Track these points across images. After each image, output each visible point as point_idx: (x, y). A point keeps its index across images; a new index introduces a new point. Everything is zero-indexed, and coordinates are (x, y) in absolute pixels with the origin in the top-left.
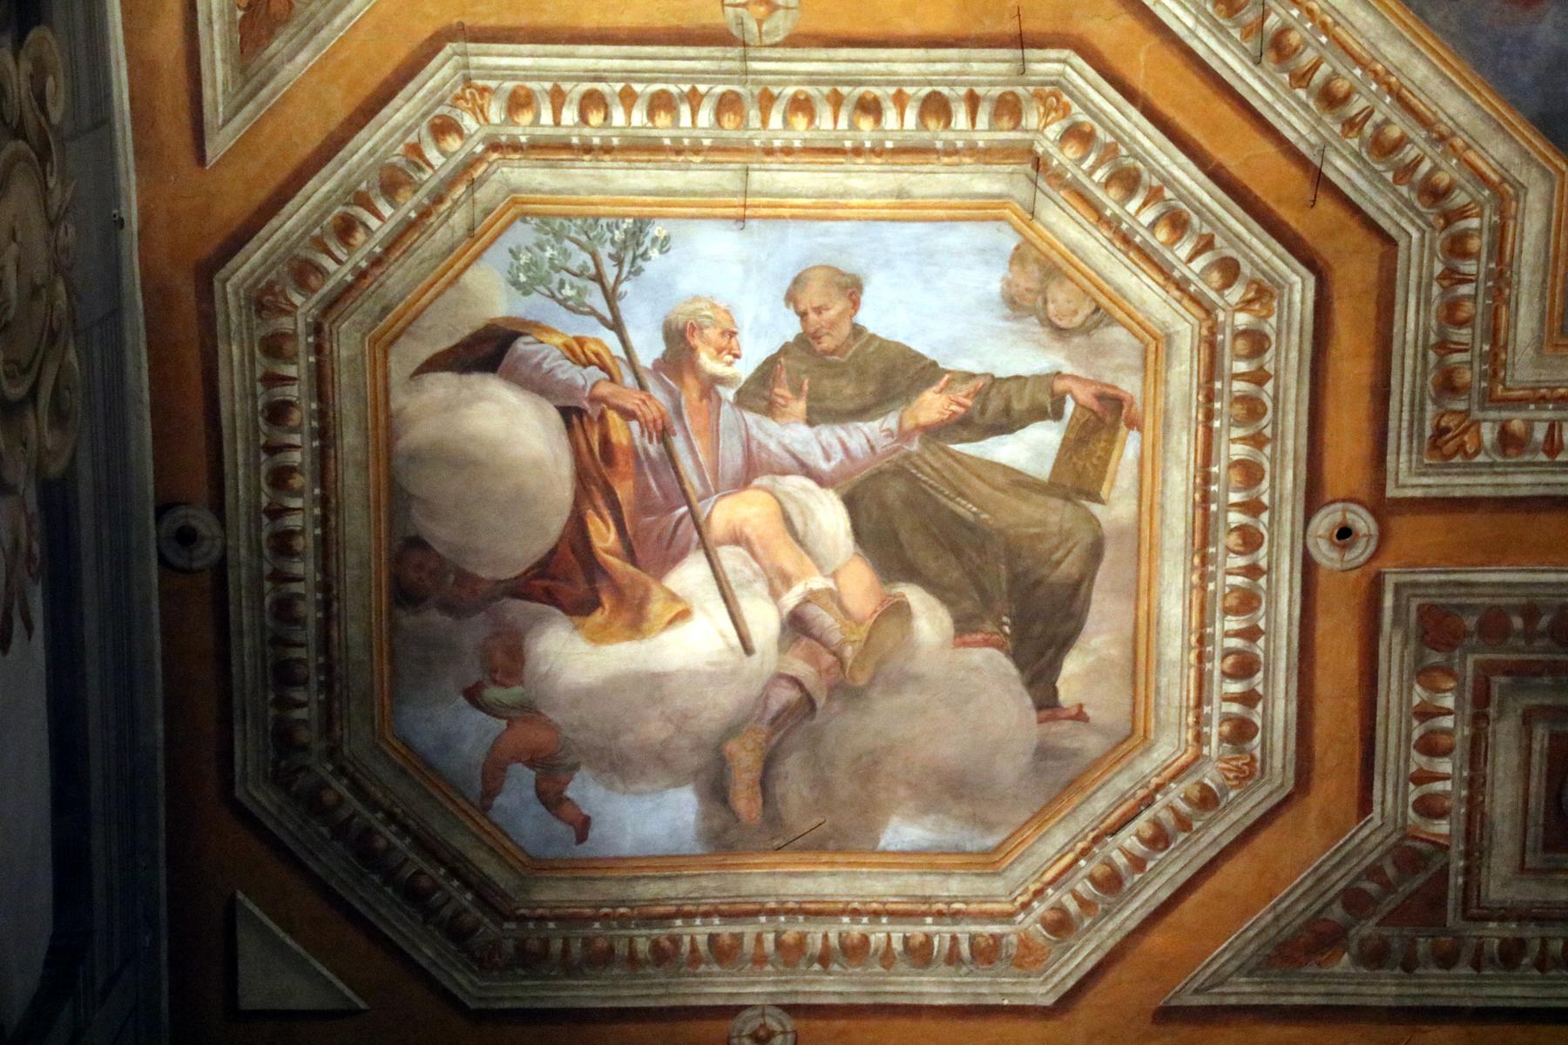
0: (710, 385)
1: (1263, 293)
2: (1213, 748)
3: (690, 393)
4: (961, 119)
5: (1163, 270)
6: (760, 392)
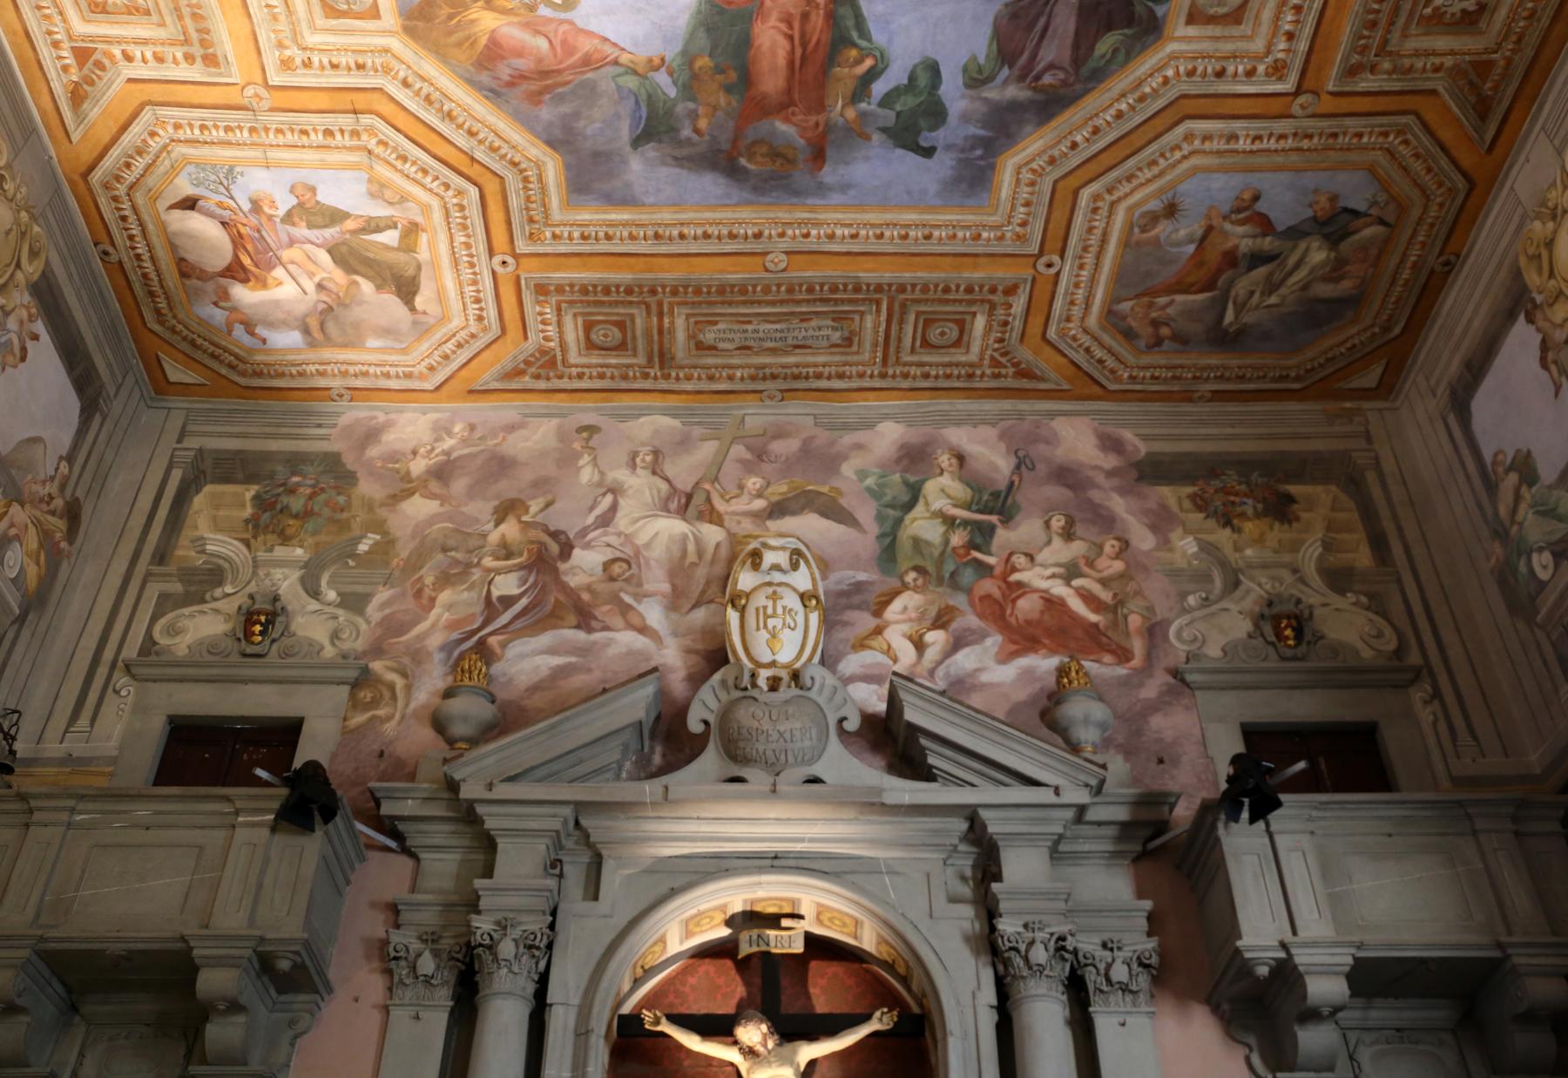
0: (270, 218)
1: (460, 193)
2: (472, 322)
3: (264, 220)
4: (338, 136)
5: (423, 186)
6: (288, 218)
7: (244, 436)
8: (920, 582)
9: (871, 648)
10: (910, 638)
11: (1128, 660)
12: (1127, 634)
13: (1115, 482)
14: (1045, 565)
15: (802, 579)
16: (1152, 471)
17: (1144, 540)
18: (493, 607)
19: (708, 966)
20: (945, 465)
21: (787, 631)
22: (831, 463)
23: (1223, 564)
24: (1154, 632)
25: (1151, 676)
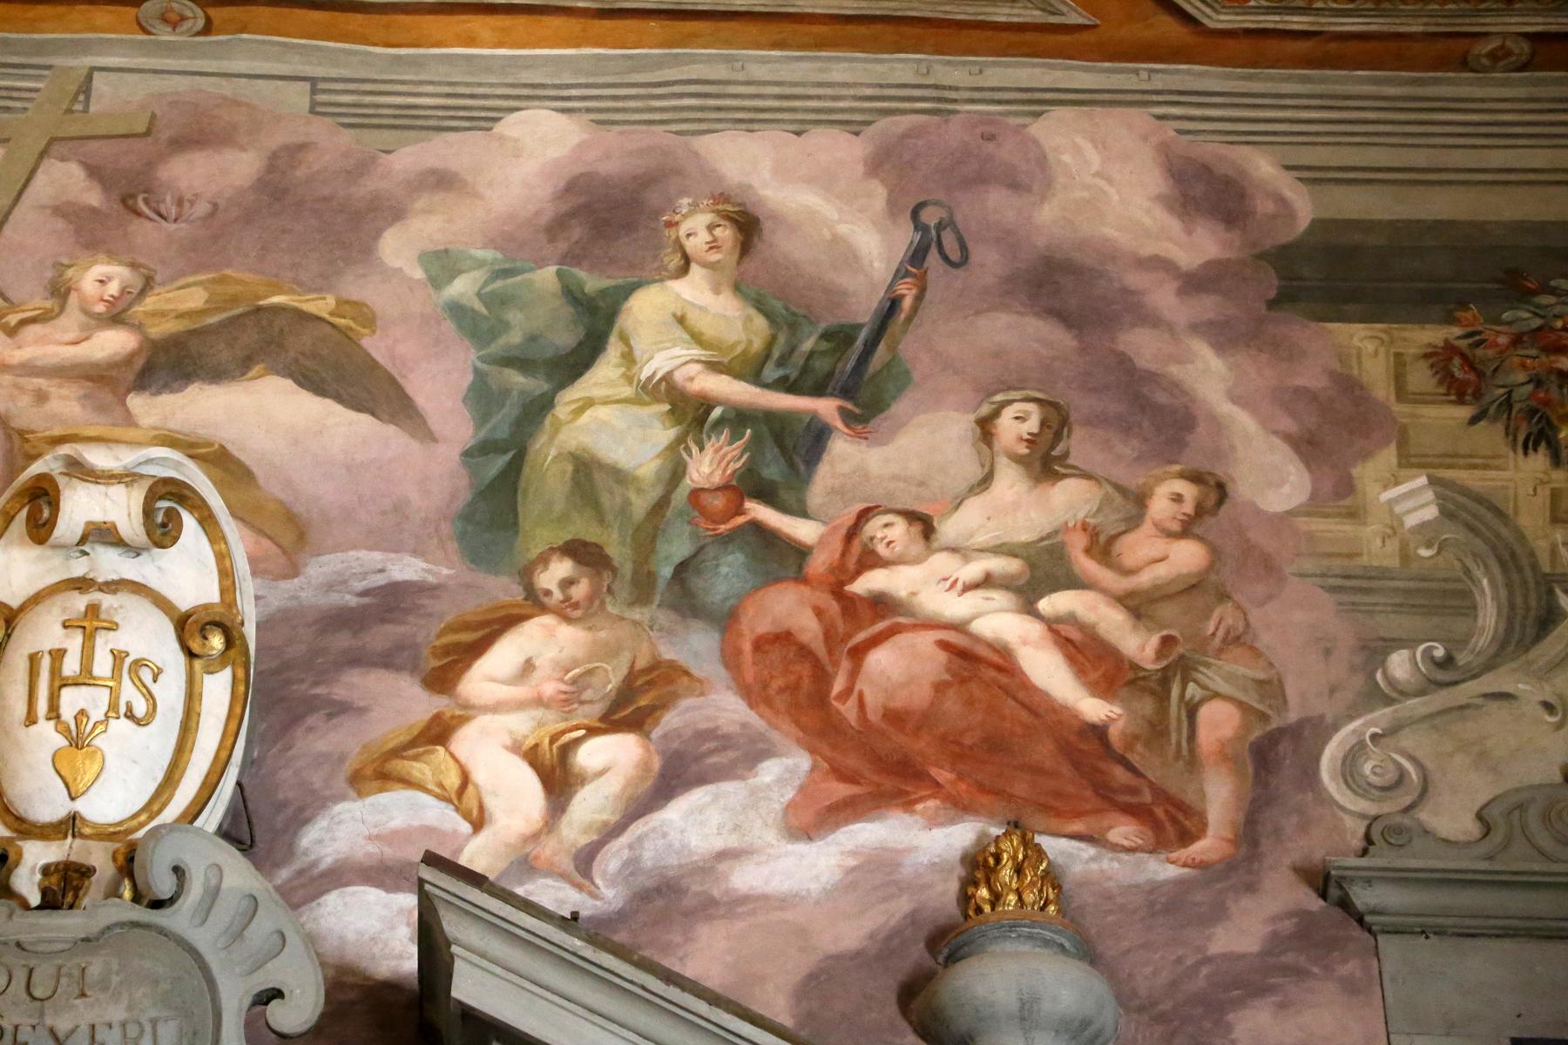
8: (580, 591)
9: (408, 783)
10: (532, 757)
11: (1186, 837)
12: (1193, 762)
13: (1208, 306)
14: (964, 545)
15: (187, 572)
16: (1323, 277)
17: (1272, 480)
20: (697, 243)
21: (121, 726)
22: (351, 226)
23: (1511, 559)
25: (1251, 888)
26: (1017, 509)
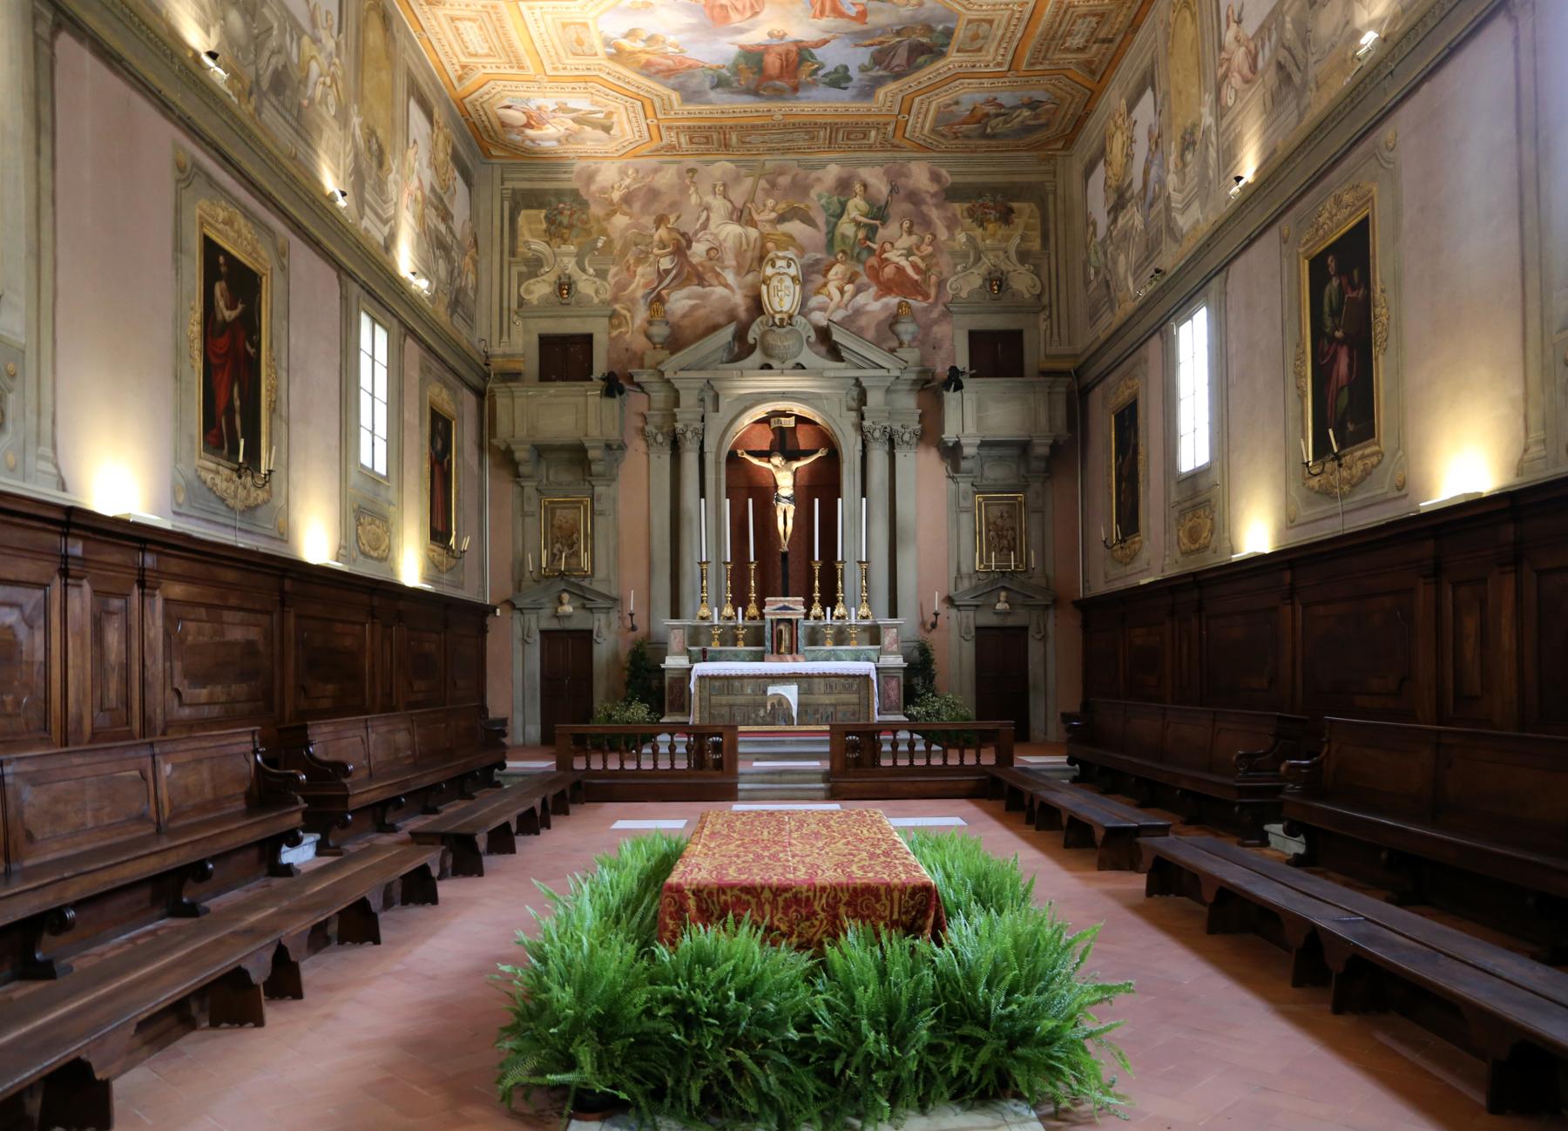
7: (530, 180)
13: (934, 201)
16: (952, 194)
17: (943, 235)
18: (661, 275)
19: (759, 426)
23: (976, 248)
24: (941, 284)
26: (906, 241)
